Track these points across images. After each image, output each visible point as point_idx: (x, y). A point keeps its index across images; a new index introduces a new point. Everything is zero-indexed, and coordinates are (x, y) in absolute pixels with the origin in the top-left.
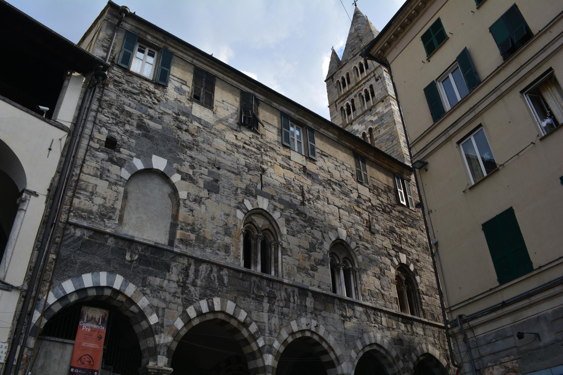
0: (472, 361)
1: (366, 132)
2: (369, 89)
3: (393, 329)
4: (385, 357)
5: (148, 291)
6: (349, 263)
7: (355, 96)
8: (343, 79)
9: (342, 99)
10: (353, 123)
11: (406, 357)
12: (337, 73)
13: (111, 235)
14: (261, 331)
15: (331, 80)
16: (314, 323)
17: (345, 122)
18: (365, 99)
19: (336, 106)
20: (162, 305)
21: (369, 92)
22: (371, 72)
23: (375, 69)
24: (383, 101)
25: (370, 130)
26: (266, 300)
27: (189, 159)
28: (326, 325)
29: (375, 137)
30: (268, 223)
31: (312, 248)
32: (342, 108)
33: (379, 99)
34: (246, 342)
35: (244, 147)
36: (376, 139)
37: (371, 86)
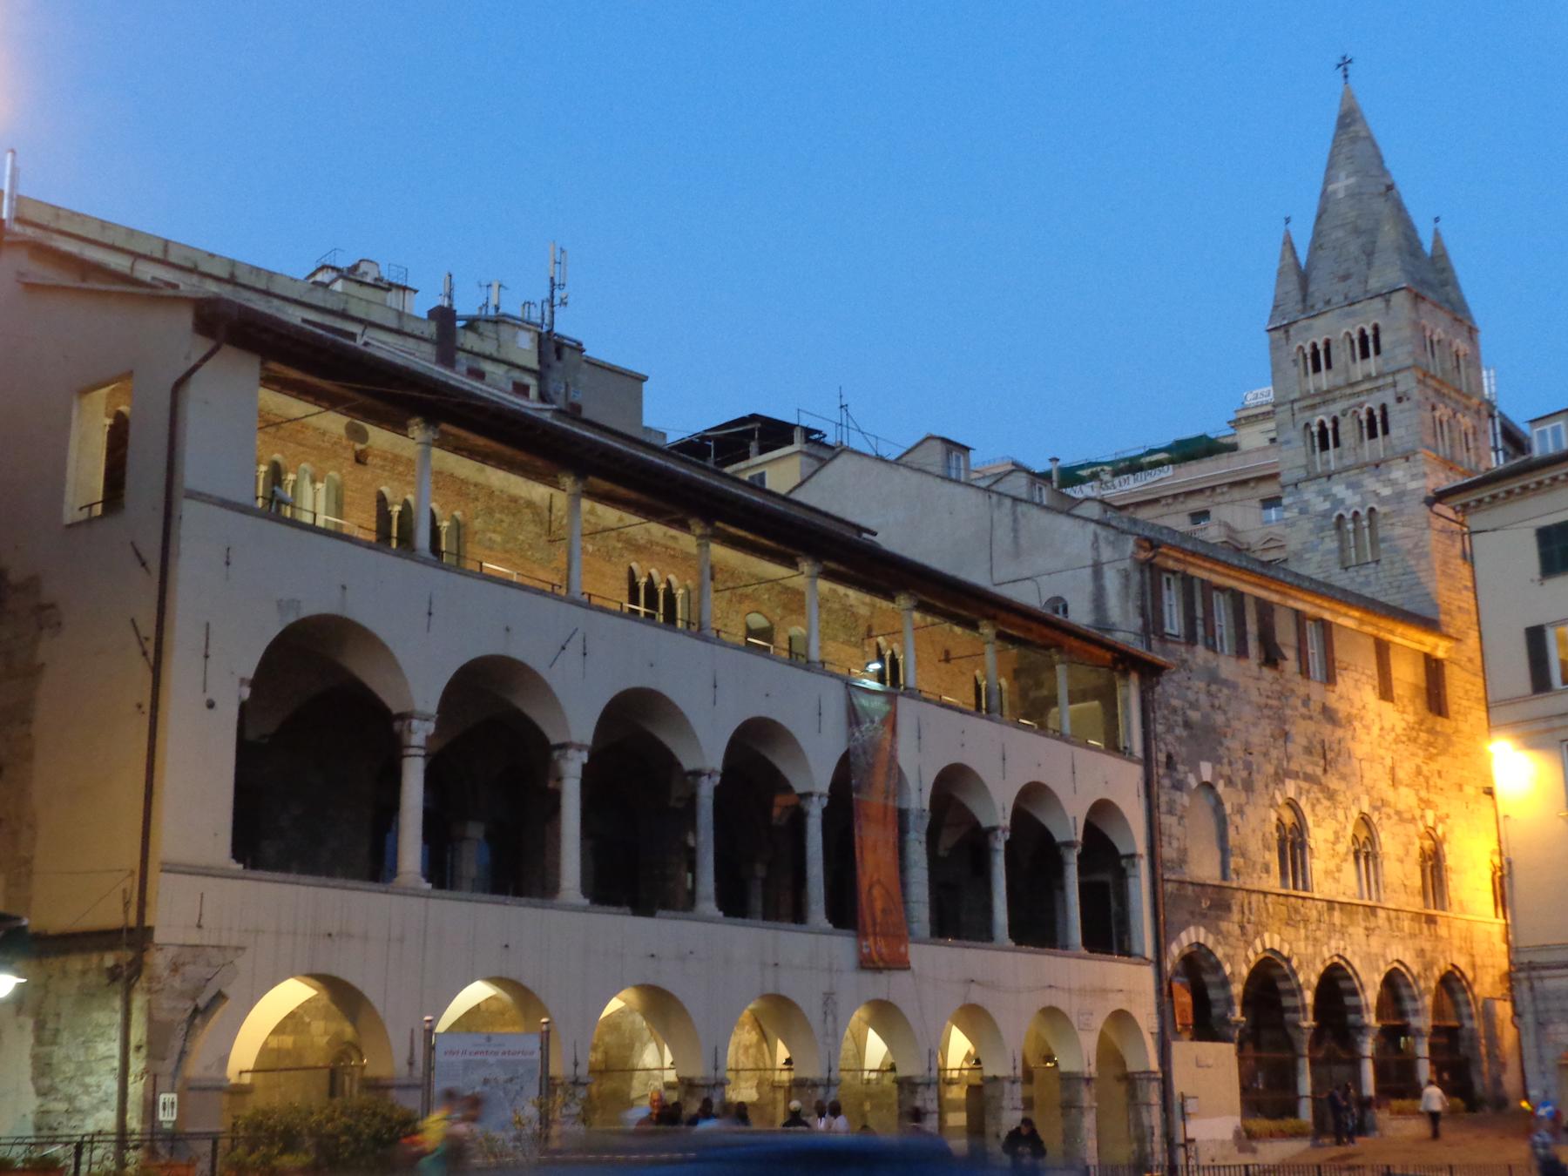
0: (1536, 1012)
1: (1363, 513)
2: (1377, 413)
3: (1415, 935)
4: (1403, 975)
5: (1221, 940)
6: (1367, 843)
7: (1344, 414)
8: (1314, 346)
9: (1309, 402)
10: (1335, 477)
11: (1428, 973)
12: (1301, 324)
13: (1192, 884)
14: (1300, 963)
15: (1279, 334)
16: (1342, 944)
17: (1314, 463)
18: (1365, 431)
19: (1293, 415)
20: (1231, 952)
21: (1378, 419)
22: (1388, 374)
23: (1399, 371)
24: (1407, 459)
25: (1372, 510)
26: (1302, 925)
27: (1227, 752)
28: (1352, 944)
29: (1381, 533)
30: (1293, 814)
31: (1337, 840)
32: (1307, 425)
33: (1399, 449)
34: (1286, 978)
35: (1266, 706)
36: (1384, 540)
37: (1384, 408)
